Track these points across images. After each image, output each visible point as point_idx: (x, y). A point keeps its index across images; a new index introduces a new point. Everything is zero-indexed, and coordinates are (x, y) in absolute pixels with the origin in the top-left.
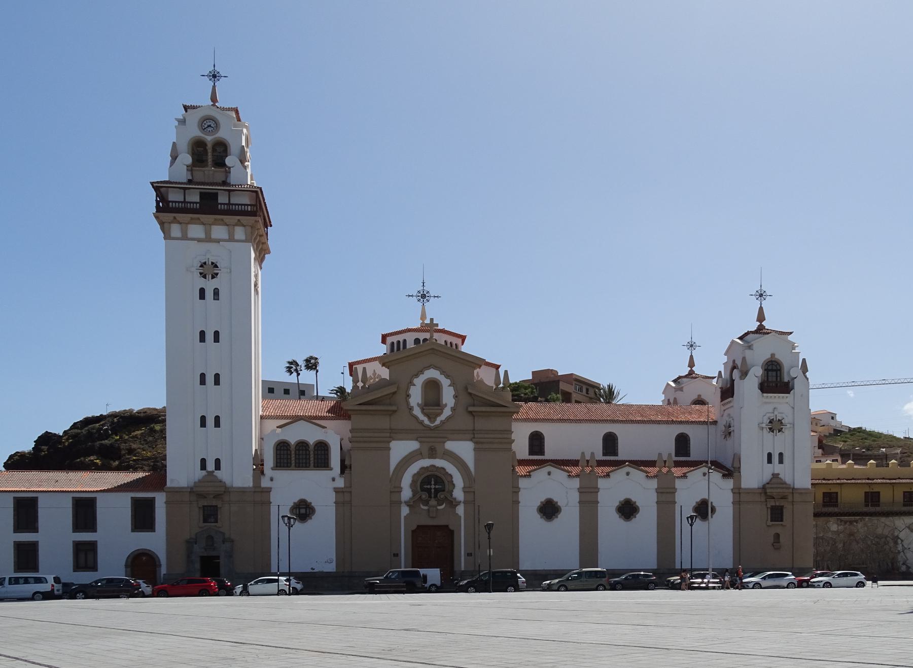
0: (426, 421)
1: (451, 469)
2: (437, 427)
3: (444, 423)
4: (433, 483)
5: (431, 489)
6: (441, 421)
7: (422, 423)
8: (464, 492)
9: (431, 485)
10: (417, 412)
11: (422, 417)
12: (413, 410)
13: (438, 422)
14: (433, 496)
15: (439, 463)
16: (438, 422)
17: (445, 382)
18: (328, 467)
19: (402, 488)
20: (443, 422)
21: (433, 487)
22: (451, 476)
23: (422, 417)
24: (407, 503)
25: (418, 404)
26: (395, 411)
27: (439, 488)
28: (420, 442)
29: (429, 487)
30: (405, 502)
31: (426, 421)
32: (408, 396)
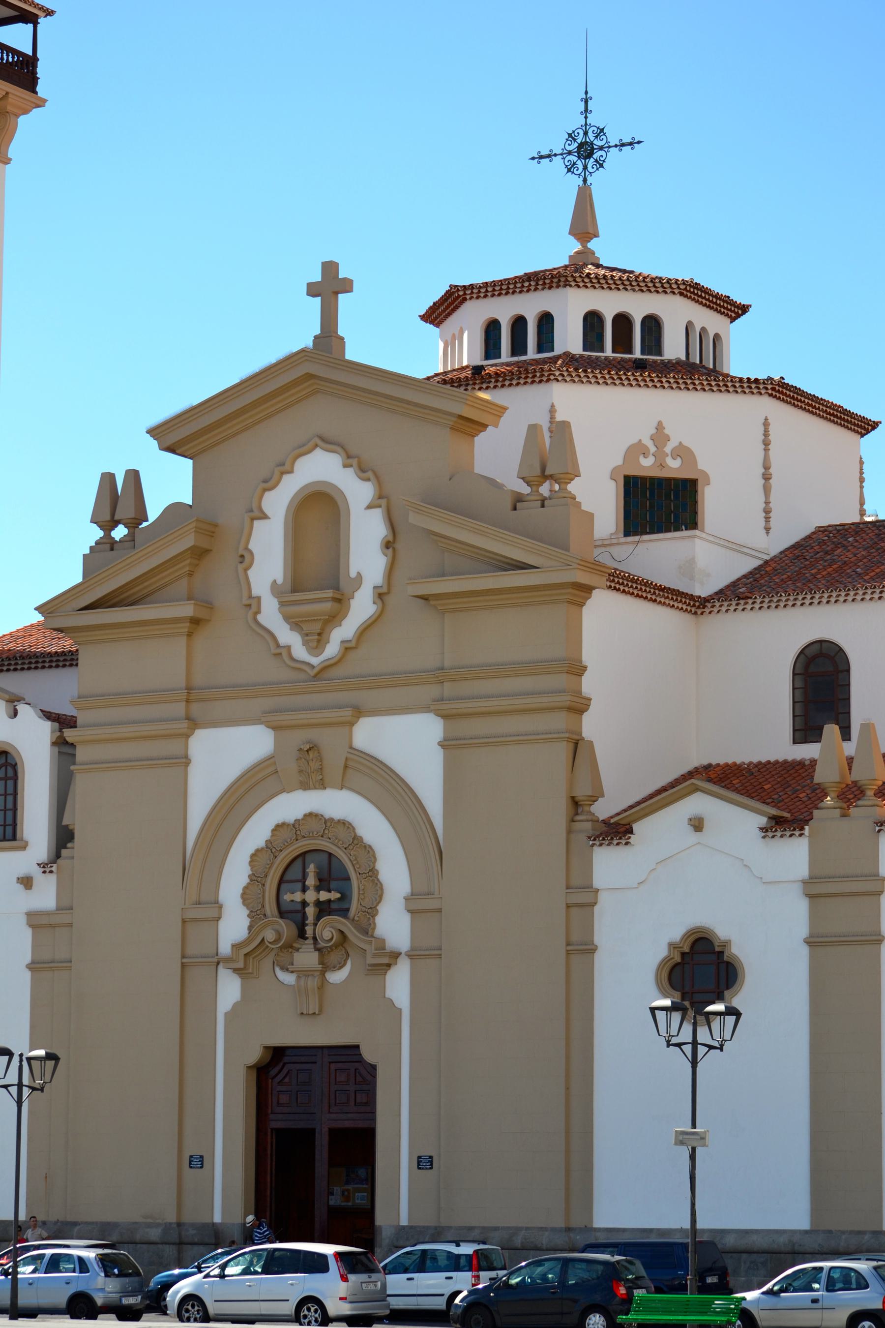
0: (300, 652)
2: (327, 667)
3: (347, 649)
4: (311, 881)
5: (318, 903)
8: (412, 912)
9: (318, 889)
11: (287, 636)
12: (258, 612)
13: (332, 649)
14: (309, 930)
16: (332, 649)
18: (14, 838)
19: (221, 907)
20: (347, 648)
21: (311, 896)
22: (369, 850)
23: (287, 636)
25: (275, 589)
26: (195, 622)
27: (329, 901)
28: (274, 728)
29: (298, 897)
31: (300, 652)
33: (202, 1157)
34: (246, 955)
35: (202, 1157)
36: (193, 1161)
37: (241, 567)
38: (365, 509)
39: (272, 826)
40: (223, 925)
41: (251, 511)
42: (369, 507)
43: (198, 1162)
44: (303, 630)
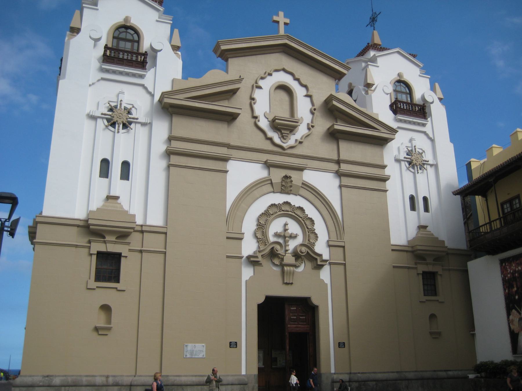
0: (277, 139)
1: (311, 211)
2: (292, 147)
3: (301, 143)
6: (296, 140)
7: (271, 139)
10: (264, 124)
11: (271, 134)
15: (296, 201)
17: (299, 92)
24: (252, 261)
30: (249, 257)
31: (277, 139)
32: (253, 99)
33: (236, 343)
34: (262, 255)
35: (236, 343)
36: (231, 344)
37: (253, 102)
38: (303, 96)
39: (270, 204)
40: (244, 243)
41: (256, 83)
42: (307, 96)
43: (234, 345)
44: (281, 132)
